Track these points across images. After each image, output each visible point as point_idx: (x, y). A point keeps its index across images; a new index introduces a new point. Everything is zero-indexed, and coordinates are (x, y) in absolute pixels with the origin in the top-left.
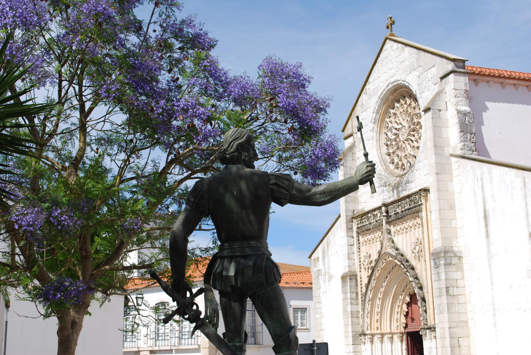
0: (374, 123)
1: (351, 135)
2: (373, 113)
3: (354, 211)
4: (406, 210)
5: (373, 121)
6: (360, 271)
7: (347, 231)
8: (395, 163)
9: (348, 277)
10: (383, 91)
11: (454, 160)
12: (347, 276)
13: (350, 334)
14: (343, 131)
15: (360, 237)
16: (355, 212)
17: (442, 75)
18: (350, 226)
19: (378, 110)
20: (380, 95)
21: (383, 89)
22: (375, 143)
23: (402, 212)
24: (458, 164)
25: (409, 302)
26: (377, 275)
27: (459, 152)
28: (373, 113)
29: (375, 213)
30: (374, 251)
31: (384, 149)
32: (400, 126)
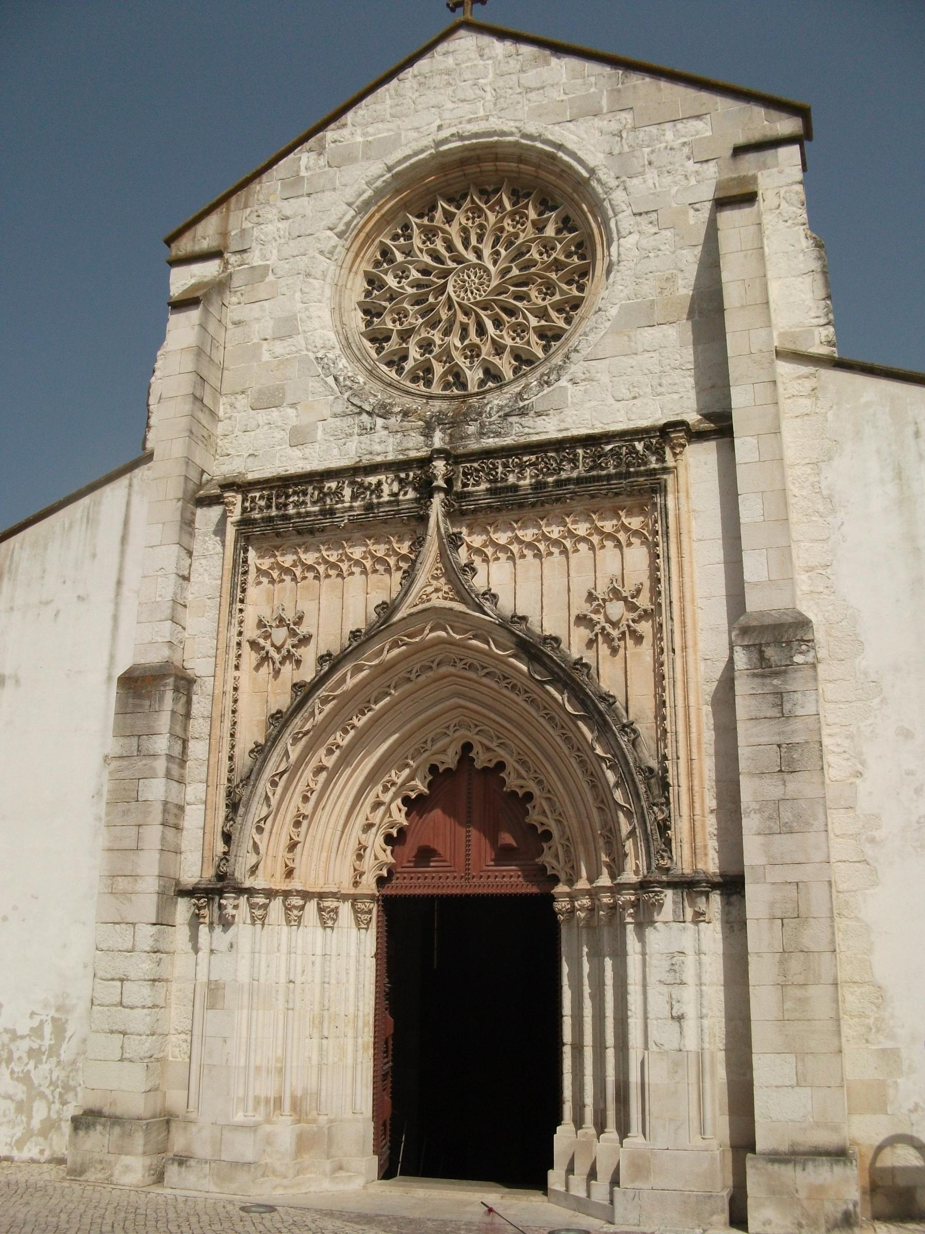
0: (340, 235)
1: (216, 254)
2: (350, 205)
3: (203, 472)
4: (559, 483)
5: (341, 227)
6: (237, 667)
7: (181, 527)
8: (409, 365)
9: (171, 680)
10: (416, 154)
11: (784, 368)
12: (164, 676)
13: (150, 885)
14: (169, 241)
15: (252, 554)
16: (205, 477)
17: (741, 140)
18: (188, 515)
19: (367, 204)
20: (399, 162)
21: (416, 146)
22: (328, 292)
23: (539, 486)
24: (808, 384)
25: (420, 796)
26: (350, 683)
27: (835, 352)
28: (350, 205)
29: (373, 480)
30: (339, 599)
31: (357, 320)
32: (471, 257)
